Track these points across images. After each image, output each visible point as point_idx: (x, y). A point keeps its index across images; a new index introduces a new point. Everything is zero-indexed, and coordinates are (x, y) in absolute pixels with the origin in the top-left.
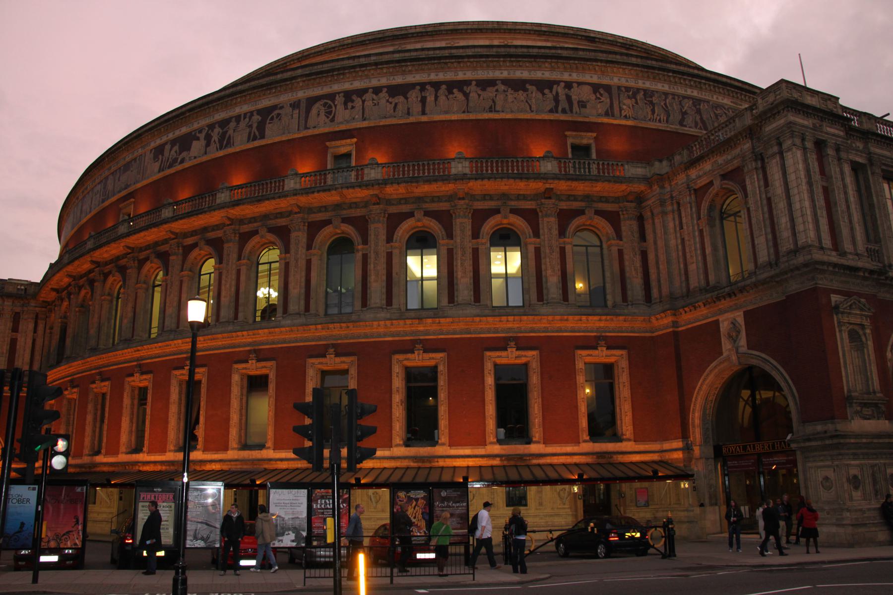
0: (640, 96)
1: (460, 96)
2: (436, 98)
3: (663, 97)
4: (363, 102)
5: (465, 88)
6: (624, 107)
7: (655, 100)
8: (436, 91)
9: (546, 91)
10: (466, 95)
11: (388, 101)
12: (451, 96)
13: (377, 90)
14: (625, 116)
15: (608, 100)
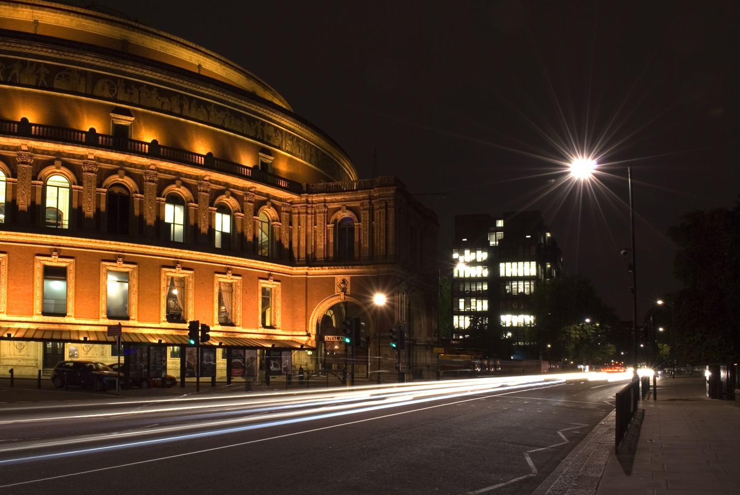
0: (295, 140)
1: (205, 111)
2: (190, 107)
3: (304, 143)
4: (140, 92)
5: (208, 106)
6: (287, 145)
7: (301, 144)
8: (190, 103)
9: (252, 124)
10: (208, 112)
11: (157, 98)
12: (199, 109)
13: (150, 88)
14: (287, 151)
15: (281, 139)
